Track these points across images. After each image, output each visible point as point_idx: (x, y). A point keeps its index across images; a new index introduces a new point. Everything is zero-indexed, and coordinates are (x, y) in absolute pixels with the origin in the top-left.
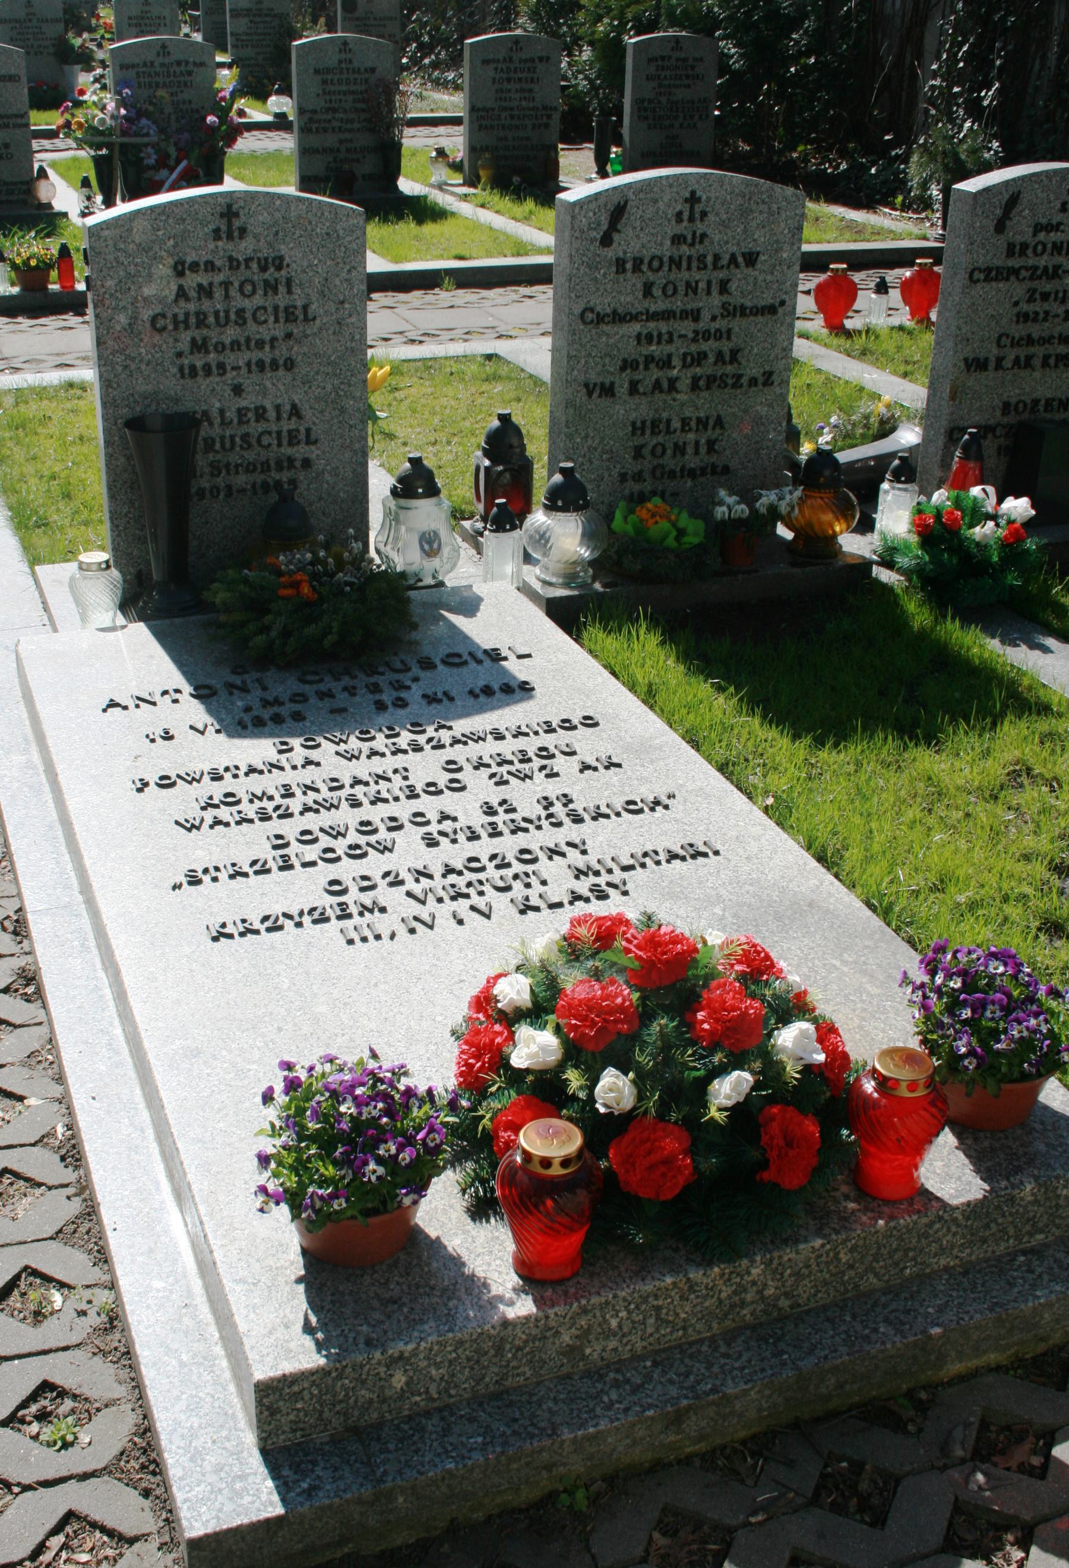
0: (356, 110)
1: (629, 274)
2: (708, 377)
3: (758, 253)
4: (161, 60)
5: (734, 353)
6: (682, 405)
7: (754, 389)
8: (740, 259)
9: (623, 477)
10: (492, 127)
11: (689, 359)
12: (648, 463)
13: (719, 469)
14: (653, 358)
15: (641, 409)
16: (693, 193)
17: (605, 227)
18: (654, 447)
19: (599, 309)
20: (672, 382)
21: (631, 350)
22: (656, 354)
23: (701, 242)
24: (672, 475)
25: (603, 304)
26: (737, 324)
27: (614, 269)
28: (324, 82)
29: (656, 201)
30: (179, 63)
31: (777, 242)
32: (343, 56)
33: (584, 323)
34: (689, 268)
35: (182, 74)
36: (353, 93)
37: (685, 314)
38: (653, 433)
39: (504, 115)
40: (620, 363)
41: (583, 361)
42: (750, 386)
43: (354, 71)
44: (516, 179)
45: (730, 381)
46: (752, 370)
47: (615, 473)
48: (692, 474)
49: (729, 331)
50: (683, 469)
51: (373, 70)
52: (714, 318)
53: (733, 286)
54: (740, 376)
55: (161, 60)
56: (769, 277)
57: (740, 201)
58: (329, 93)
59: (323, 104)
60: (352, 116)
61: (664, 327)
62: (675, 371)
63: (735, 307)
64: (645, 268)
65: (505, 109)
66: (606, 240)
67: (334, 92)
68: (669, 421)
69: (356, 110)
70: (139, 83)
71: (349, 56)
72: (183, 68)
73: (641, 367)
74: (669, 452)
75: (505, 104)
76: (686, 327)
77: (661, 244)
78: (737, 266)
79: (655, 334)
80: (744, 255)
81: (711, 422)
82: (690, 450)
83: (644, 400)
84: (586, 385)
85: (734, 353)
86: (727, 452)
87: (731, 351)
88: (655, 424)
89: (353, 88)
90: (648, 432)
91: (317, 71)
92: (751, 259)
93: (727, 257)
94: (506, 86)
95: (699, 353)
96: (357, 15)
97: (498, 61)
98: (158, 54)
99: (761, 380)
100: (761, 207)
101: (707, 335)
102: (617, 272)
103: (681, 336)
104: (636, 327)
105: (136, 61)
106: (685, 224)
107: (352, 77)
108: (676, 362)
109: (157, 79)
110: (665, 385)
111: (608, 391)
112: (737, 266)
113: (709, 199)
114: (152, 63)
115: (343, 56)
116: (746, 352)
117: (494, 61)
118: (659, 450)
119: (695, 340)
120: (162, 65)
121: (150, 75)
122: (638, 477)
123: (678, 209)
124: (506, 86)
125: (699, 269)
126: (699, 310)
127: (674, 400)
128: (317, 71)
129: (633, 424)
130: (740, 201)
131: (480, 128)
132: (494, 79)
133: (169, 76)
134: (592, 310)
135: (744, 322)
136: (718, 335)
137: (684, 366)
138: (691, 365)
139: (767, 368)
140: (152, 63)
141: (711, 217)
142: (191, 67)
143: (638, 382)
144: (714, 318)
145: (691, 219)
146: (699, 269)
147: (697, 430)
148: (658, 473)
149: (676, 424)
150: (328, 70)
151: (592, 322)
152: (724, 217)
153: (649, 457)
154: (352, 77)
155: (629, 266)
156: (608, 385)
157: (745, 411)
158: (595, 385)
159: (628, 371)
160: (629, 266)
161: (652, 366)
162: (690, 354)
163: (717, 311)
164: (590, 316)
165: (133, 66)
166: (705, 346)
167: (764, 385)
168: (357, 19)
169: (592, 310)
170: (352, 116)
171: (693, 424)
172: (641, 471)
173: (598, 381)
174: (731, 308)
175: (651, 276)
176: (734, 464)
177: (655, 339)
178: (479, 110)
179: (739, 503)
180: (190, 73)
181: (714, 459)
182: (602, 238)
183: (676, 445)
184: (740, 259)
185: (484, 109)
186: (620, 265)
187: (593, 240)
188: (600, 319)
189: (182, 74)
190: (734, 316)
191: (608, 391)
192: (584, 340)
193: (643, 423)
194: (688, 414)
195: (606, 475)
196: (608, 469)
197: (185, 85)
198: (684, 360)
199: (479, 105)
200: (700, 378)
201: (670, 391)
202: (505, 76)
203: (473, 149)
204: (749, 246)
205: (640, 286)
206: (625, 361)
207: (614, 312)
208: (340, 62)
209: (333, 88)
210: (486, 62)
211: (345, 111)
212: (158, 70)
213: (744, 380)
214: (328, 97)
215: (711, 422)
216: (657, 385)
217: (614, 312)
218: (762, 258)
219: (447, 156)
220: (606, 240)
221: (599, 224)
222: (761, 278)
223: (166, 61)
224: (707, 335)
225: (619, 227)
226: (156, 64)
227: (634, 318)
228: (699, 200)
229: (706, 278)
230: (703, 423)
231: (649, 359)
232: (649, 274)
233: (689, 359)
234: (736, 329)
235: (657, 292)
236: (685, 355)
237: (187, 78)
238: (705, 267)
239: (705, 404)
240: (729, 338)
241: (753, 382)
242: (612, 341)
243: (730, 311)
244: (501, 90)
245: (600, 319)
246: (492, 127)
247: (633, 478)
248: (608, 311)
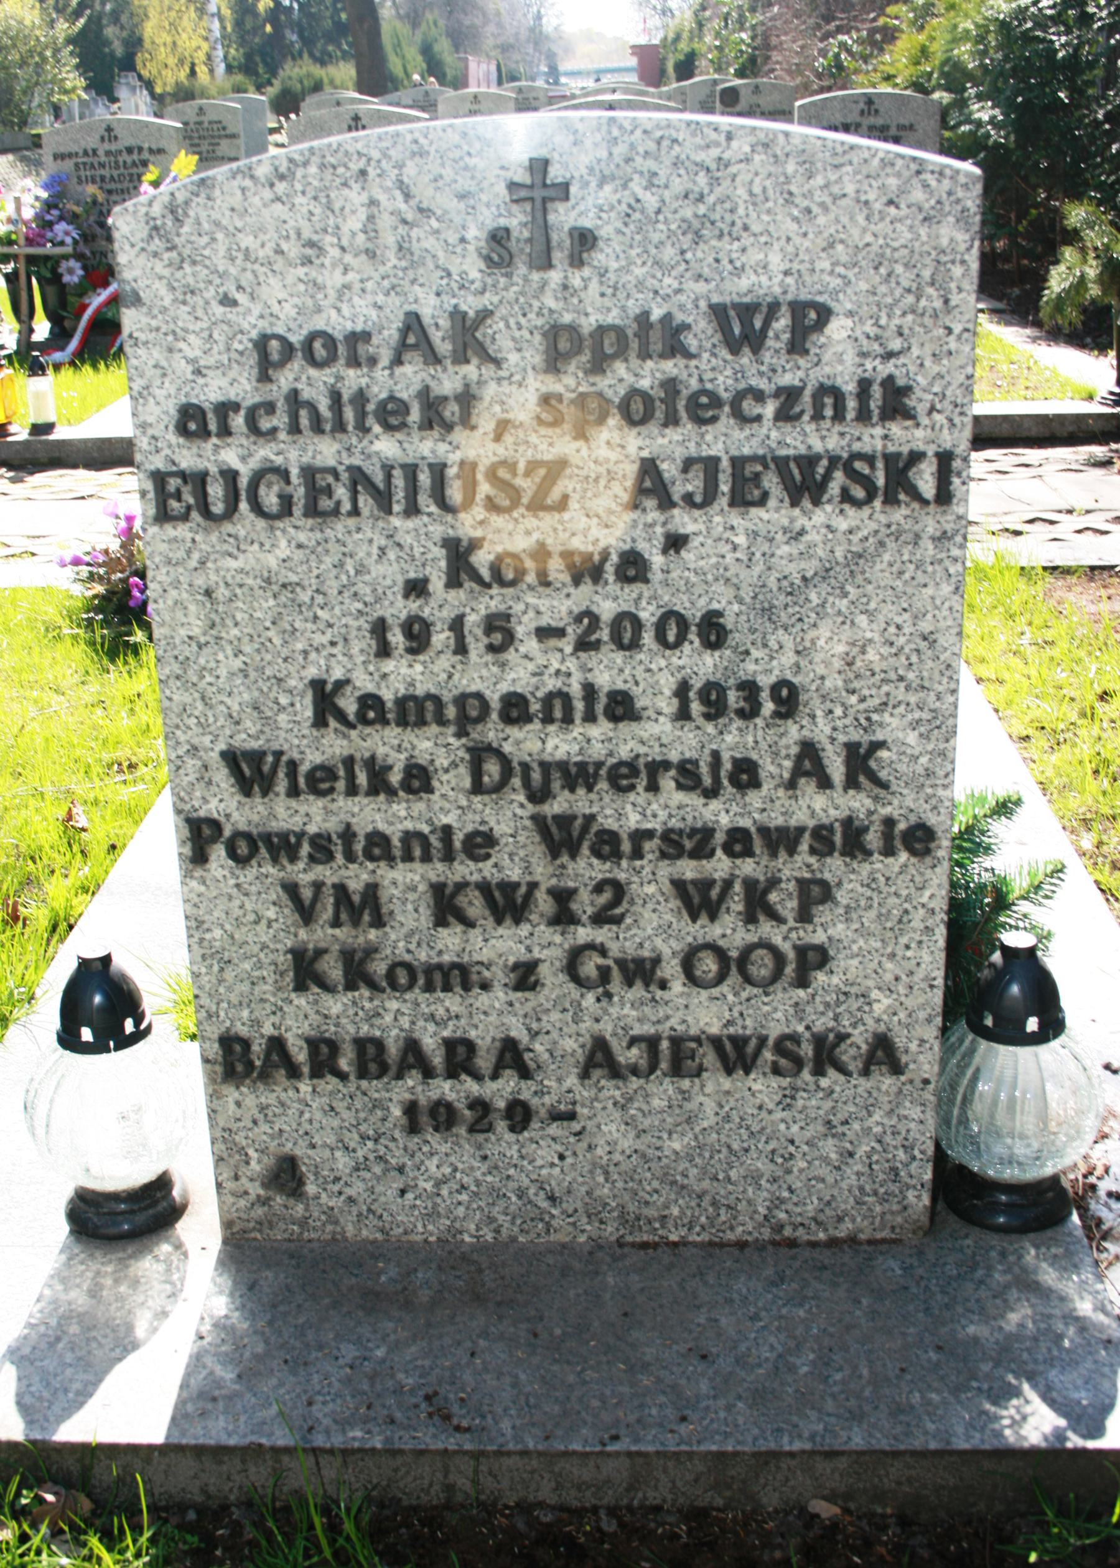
30: (130, 150)
35: (134, 164)
55: (107, 146)
72: (135, 157)
98: (102, 139)
105: (74, 148)
114: (94, 151)
120: (108, 153)
121: (92, 166)
133: (117, 167)
140: (94, 151)
142: (145, 155)
165: (70, 155)
189: (134, 164)
212: (103, 159)
223: (113, 147)
226: (101, 152)
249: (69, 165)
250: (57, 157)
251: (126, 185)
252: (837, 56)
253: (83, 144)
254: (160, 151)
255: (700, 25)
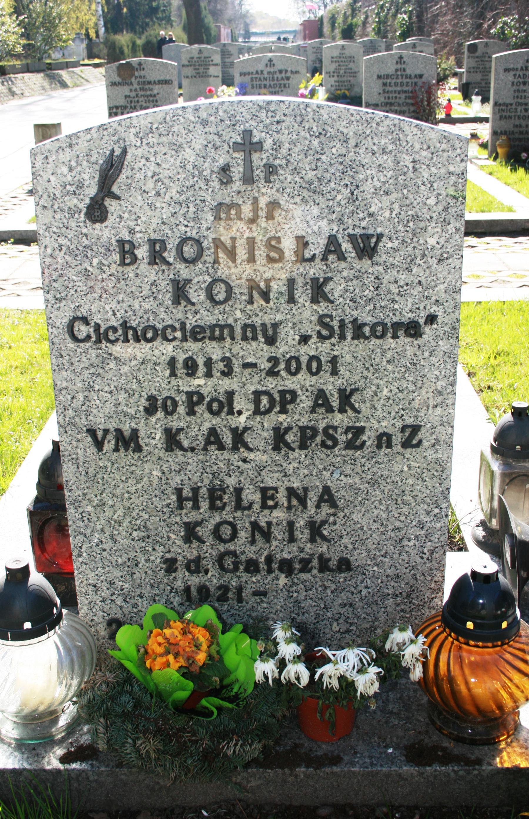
0: (407, 104)
1: (144, 267)
2: (303, 429)
3: (380, 237)
4: (268, 69)
5: (346, 398)
6: (260, 469)
7: (385, 450)
8: (346, 246)
9: (170, 565)
10: (510, 117)
11: (265, 400)
12: (210, 550)
13: (333, 564)
14: (202, 398)
15: (193, 470)
16: (247, 134)
17: (93, 191)
18: (218, 526)
19: (97, 319)
20: (239, 437)
21: (161, 384)
22: (205, 391)
23: (270, 217)
24: (252, 566)
25: (105, 312)
26: (347, 350)
27: (116, 257)
28: (385, 84)
29: (178, 148)
30: (281, 72)
31: (415, 218)
32: (399, 66)
33: (75, 339)
34: (252, 259)
36: (405, 92)
37: (250, 332)
38: (213, 507)
39: (519, 109)
40: (143, 402)
41: (81, 397)
42: (379, 446)
43: (406, 77)
44: (524, 155)
45: (342, 438)
46: (379, 420)
47: (157, 557)
48: (286, 567)
49: (334, 361)
50: (269, 560)
51: (421, 76)
52: (305, 339)
53: (336, 289)
54: (360, 431)
55: (268, 69)
56: (403, 278)
57: (338, 148)
58: (388, 92)
59: (383, 100)
60: (404, 108)
61: (215, 351)
62: (242, 419)
63: (342, 324)
64: (170, 256)
65: (521, 104)
66: (96, 212)
67: (391, 92)
68: (238, 491)
69: (407, 104)
70: (252, 85)
71: (403, 66)
72: (283, 75)
73: (181, 409)
74: (242, 534)
75: (520, 101)
76: (258, 352)
77: (196, 219)
78: (342, 257)
79: (201, 361)
80: (352, 238)
81: (313, 498)
82: (278, 533)
83: (192, 459)
84: (92, 432)
85: (346, 398)
86: (345, 540)
87: (341, 391)
88: (215, 495)
89: (405, 88)
90: (204, 505)
91: (379, 77)
92: (366, 247)
93: (323, 241)
94: (522, 87)
95: (282, 393)
96: (477, 54)
97: (517, 69)
98: (267, 65)
99: (397, 439)
100: (382, 159)
101: (293, 366)
102: (123, 263)
103: (246, 366)
104: (166, 350)
105: (251, 70)
106: (237, 185)
107: (405, 81)
108: (240, 403)
109: (265, 82)
110: (227, 439)
111: (128, 441)
112: (342, 257)
113: (277, 146)
114: (262, 72)
115: (399, 66)
116: (368, 393)
117: (513, 69)
118: (226, 531)
119: (272, 373)
120: (269, 73)
121: (260, 79)
122: (195, 566)
123: (221, 162)
124: (522, 87)
125: (271, 260)
126: (275, 326)
127: (245, 461)
128: (379, 77)
129: (179, 491)
130: (338, 148)
131: (501, 117)
132: (513, 83)
134: (85, 320)
135: (361, 348)
136: (315, 366)
137: (257, 412)
138: (268, 411)
139: (410, 421)
140: (262, 72)
141: (286, 176)
142: (289, 74)
143: (180, 430)
144: (305, 339)
145: (248, 179)
146: (271, 260)
147: (289, 507)
148: (228, 562)
149: (250, 495)
150: (388, 76)
151: (88, 338)
152: (311, 175)
153: (210, 540)
154: (405, 81)
155: (142, 252)
156: (127, 433)
157: (373, 483)
158: (106, 431)
159: (160, 414)
160: (142, 252)
161: (200, 409)
162: (267, 393)
163: (311, 328)
164: (82, 330)
165: (249, 74)
166: (290, 383)
167: (406, 444)
168: (477, 57)
169: (85, 320)
170: (404, 108)
171: (282, 497)
172: (198, 559)
173: (112, 426)
174: (335, 324)
175: (184, 271)
176: (358, 558)
177: (202, 369)
178: (500, 105)
179: (297, 659)
180: (288, 78)
181: (323, 548)
182: (90, 208)
183: (255, 526)
184: (346, 246)
185: (505, 104)
186: (126, 251)
187: (72, 212)
188: (101, 336)
190: (342, 337)
191: (128, 441)
192: (79, 367)
193: (195, 490)
194: (271, 483)
195: (142, 559)
196: (144, 551)
197: (285, 86)
198: (257, 402)
199: (501, 101)
200: (289, 429)
201: (235, 448)
202: (521, 80)
203: (495, 133)
204: (360, 225)
205: (164, 284)
206: (152, 399)
207: (125, 325)
208: (397, 70)
209: (390, 89)
210: (507, 70)
211: (399, 105)
212: (266, 76)
213: (369, 438)
214: (387, 95)
215: (313, 498)
216: (213, 438)
217: (125, 325)
218: (386, 244)
219: (478, 138)
220: (96, 212)
221: (80, 186)
222: (387, 278)
223: (272, 70)
224: (293, 366)
225: (115, 189)
226: (265, 72)
227: (162, 334)
228: (259, 146)
229: (284, 276)
230: (296, 496)
231: (194, 400)
232: (181, 266)
233: (265, 400)
234: (348, 358)
235: (197, 295)
236: (257, 394)
237: (286, 82)
238: (281, 258)
239: (300, 469)
240: (334, 372)
241: (384, 440)
242: (125, 369)
243: (327, 329)
244: (518, 91)
245: (101, 336)
246: (510, 117)
247: (188, 567)
248: (114, 322)
249: (247, 78)
250: (242, 74)
251: (277, 89)
252: (502, 28)
253: (256, 68)
254: (297, 72)
255: (354, 10)
